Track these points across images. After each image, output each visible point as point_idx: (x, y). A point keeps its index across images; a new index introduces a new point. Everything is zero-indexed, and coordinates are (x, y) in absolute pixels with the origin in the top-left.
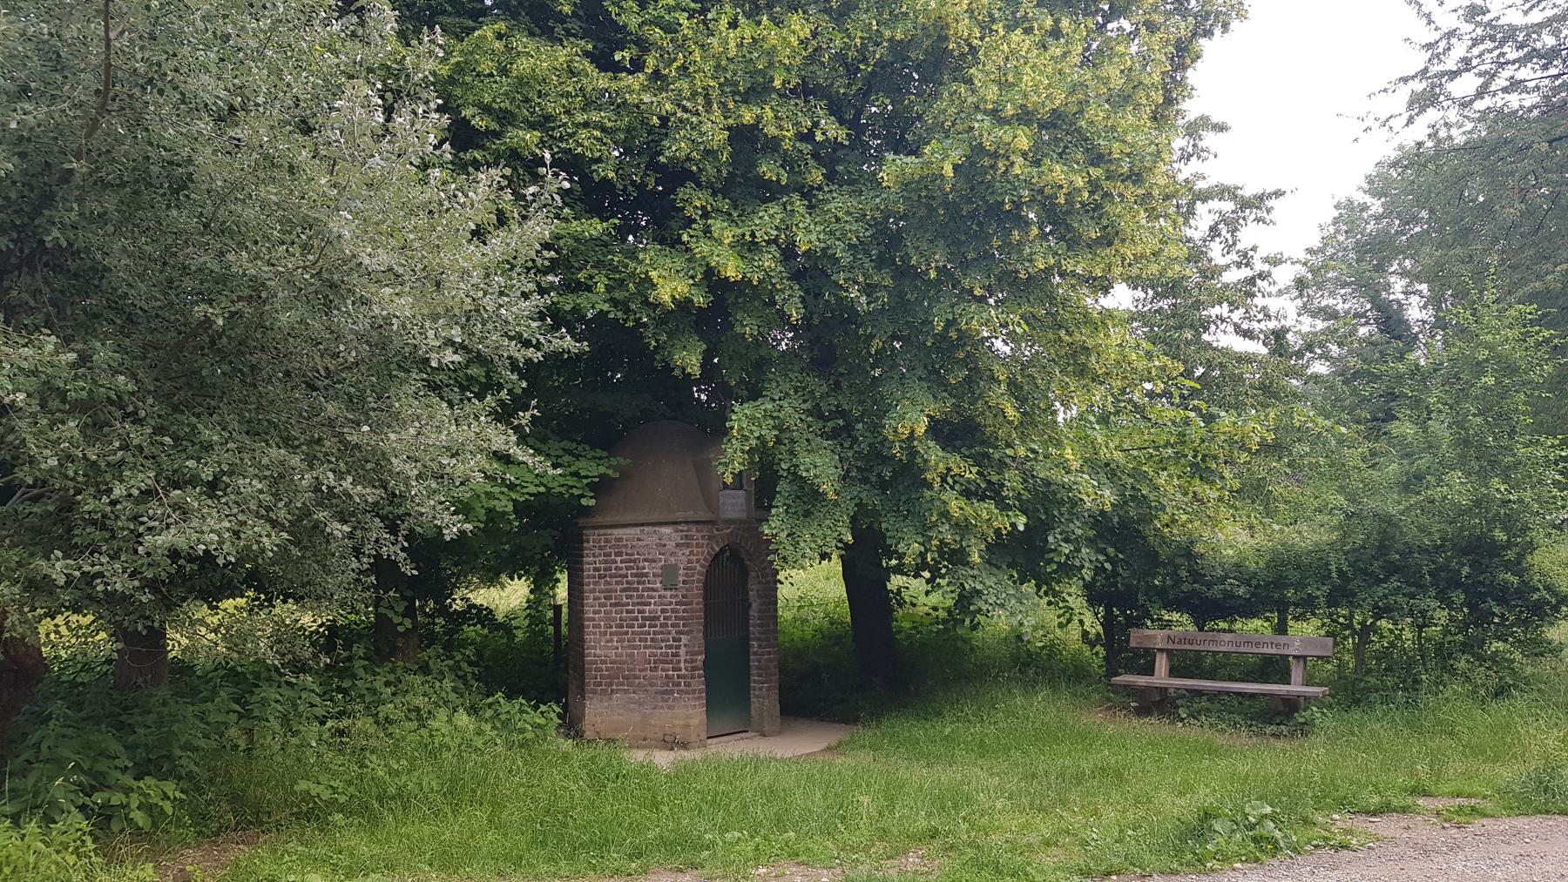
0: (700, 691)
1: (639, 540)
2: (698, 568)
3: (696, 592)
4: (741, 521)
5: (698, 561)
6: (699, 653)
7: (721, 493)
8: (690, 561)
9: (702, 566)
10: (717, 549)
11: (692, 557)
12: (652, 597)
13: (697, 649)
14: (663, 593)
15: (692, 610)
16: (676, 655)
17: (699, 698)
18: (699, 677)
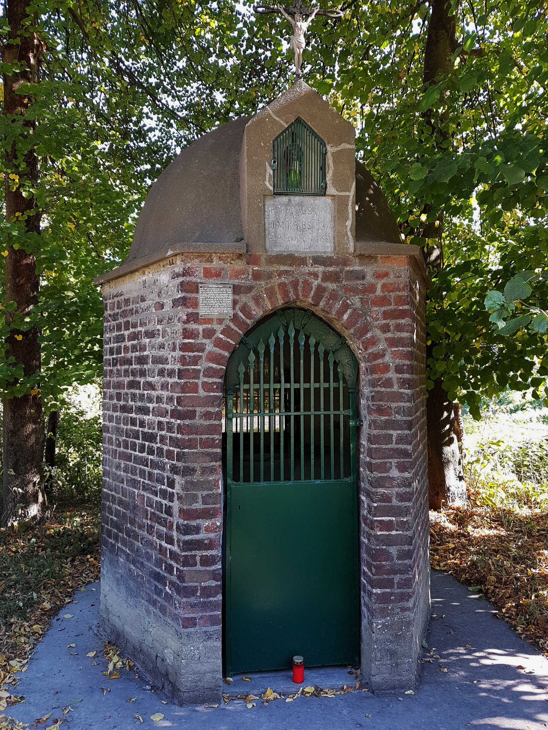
0: (207, 592)
1: (143, 300)
2: (210, 347)
3: (202, 393)
4: (318, 260)
5: (209, 334)
6: (207, 514)
7: (269, 202)
8: (187, 334)
9: (218, 343)
10: (258, 313)
11: (193, 326)
12: (150, 400)
13: (198, 505)
14: (159, 392)
15: (191, 430)
16: (169, 511)
17: (205, 606)
18: (207, 561)
